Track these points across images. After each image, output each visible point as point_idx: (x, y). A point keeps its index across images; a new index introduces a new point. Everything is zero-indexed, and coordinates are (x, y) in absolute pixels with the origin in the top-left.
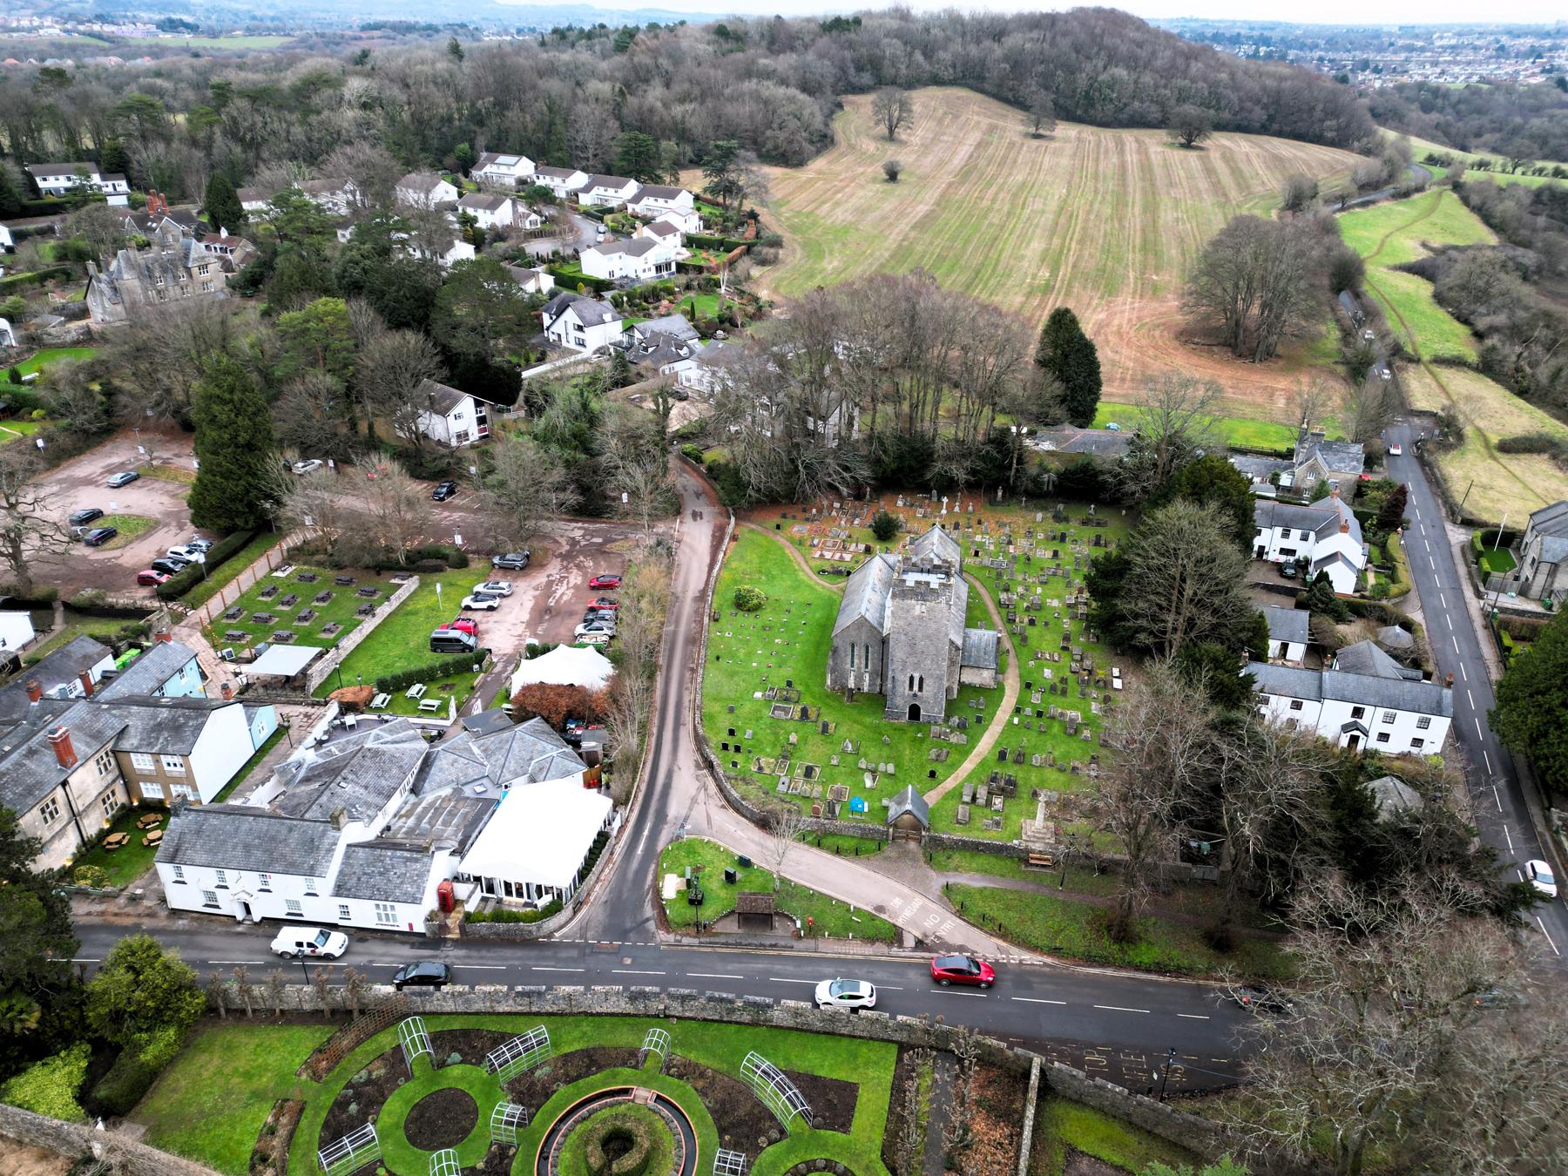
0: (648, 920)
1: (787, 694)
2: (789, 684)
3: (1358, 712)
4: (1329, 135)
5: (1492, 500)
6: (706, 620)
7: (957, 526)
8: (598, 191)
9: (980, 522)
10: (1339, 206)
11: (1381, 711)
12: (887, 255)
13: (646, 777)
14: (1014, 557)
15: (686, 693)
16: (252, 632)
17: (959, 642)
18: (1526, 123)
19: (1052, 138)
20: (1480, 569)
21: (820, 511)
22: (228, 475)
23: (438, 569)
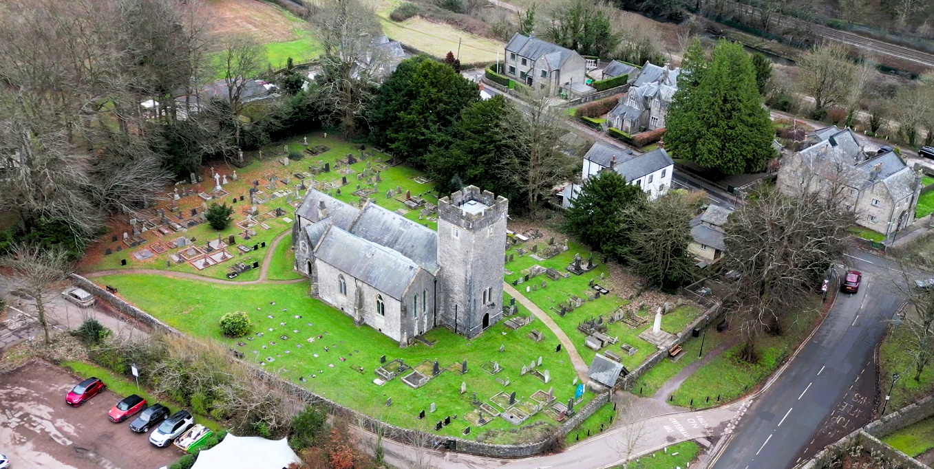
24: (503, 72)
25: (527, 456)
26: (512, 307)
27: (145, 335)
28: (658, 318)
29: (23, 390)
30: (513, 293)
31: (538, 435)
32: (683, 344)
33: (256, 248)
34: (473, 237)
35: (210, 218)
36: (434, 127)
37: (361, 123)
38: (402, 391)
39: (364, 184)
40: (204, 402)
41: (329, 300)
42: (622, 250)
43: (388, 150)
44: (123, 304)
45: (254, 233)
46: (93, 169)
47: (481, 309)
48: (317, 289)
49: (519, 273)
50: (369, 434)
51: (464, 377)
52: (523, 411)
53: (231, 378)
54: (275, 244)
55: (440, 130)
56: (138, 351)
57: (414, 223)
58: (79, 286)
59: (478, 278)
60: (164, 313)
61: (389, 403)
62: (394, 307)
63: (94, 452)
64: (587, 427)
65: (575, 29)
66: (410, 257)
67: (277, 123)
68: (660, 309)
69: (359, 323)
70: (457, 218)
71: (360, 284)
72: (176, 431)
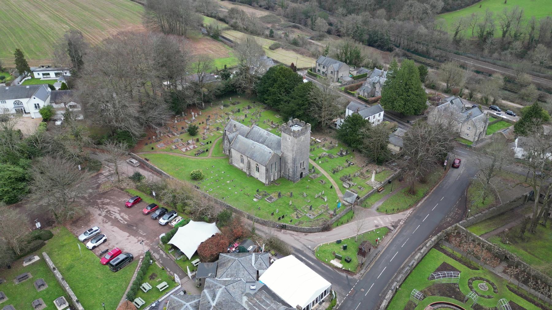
0: (347, 277)
2: (258, 191)
24: (315, 72)
25: (316, 232)
26: (312, 170)
27: (159, 179)
28: (373, 176)
29: (108, 200)
30: (314, 164)
31: (321, 223)
32: (384, 187)
33: (207, 143)
34: (296, 140)
35: (189, 131)
36: (283, 94)
37: (254, 92)
38: (265, 204)
39: (254, 117)
40: (182, 207)
41: (237, 165)
42: (360, 147)
43: (265, 103)
44: (151, 166)
45: (207, 137)
46: (141, 110)
47: (299, 170)
48: (232, 161)
49: (317, 156)
50: (250, 222)
51: (291, 198)
52: (315, 213)
53: (193, 198)
54: (215, 142)
55: (286, 95)
56: (156, 185)
57: (272, 134)
58: (134, 158)
59: (298, 157)
60: (168, 170)
61: (259, 209)
62: (263, 169)
63: (136, 227)
64: (341, 220)
65: (346, 54)
66: (270, 148)
67: (218, 91)
68: (374, 172)
69: (249, 175)
70: (290, 132)
71: (249, 159)
72: (170, 219)
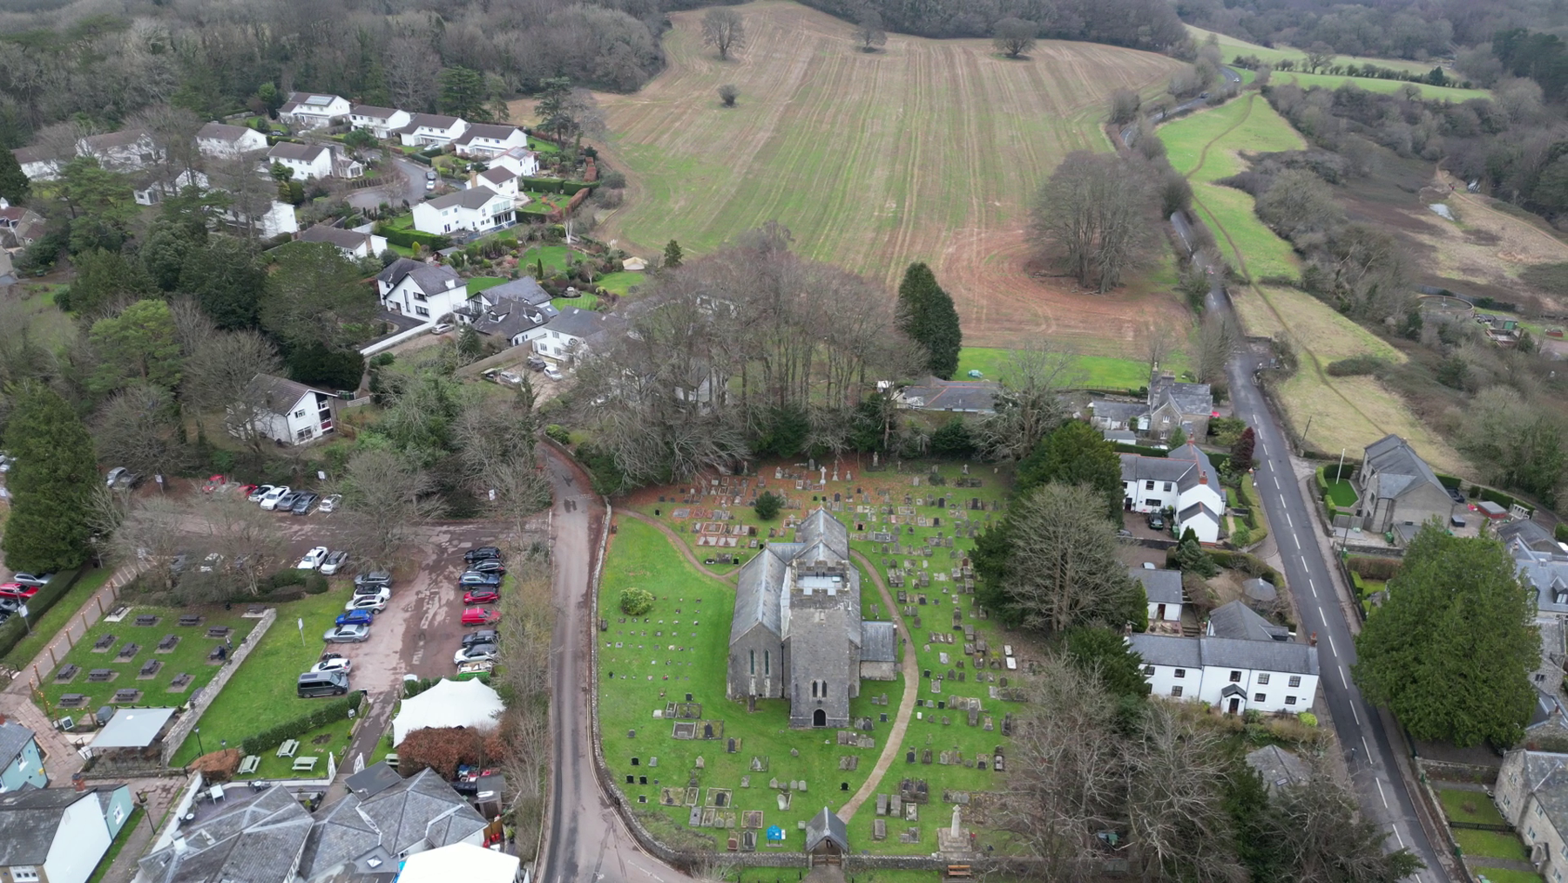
1: (686, 711)
2: (689, 697)
3: (1235, 676)
4: (1144, 39)
5: (1329, 429)
6: (594, 630)
7: (837, 498)
8: (423, 131)
9: (859, 491)
10: (1160, 115)
11: (1256, 674)
12: (733, 190)
13: (550, 823)
14: (897, 529)
15: (581, 718)
16: (91, 693)
17: (857, 640)
18: (1319, 18)
19: (883, 52)
20: (1326, 506)
21: (698, 491)
22: (47, 513)
23: (296, 597)
